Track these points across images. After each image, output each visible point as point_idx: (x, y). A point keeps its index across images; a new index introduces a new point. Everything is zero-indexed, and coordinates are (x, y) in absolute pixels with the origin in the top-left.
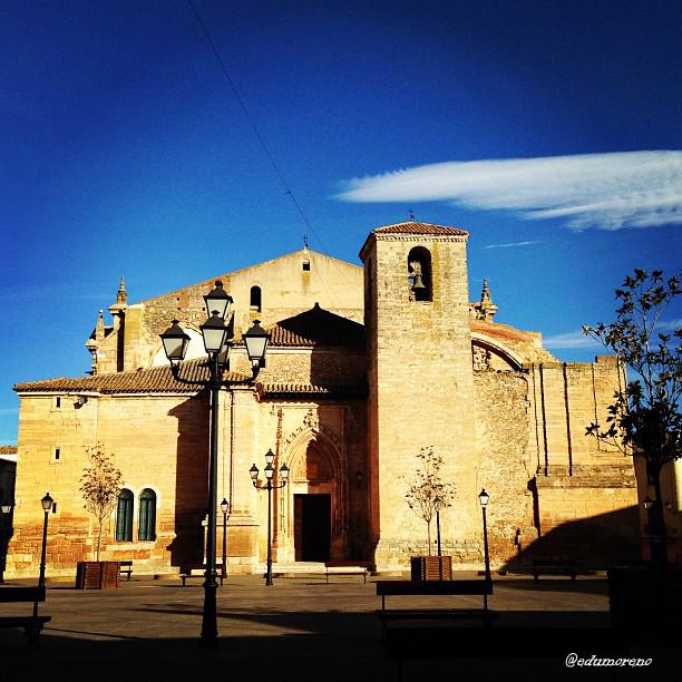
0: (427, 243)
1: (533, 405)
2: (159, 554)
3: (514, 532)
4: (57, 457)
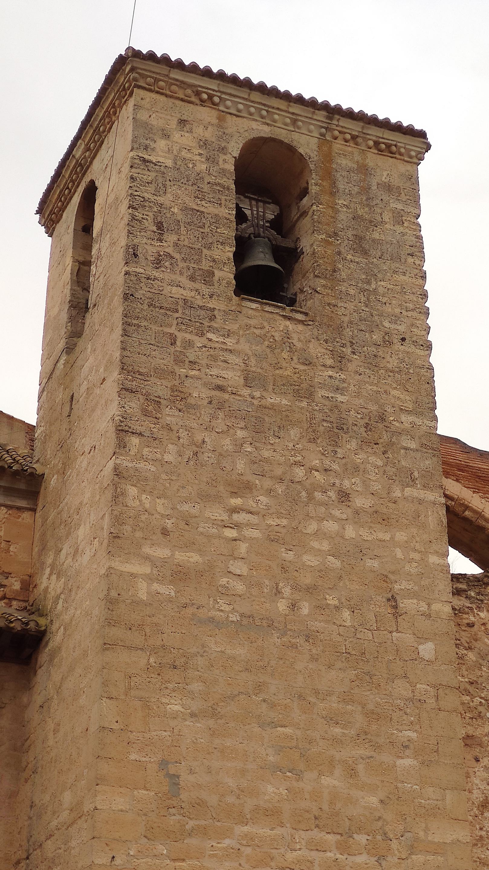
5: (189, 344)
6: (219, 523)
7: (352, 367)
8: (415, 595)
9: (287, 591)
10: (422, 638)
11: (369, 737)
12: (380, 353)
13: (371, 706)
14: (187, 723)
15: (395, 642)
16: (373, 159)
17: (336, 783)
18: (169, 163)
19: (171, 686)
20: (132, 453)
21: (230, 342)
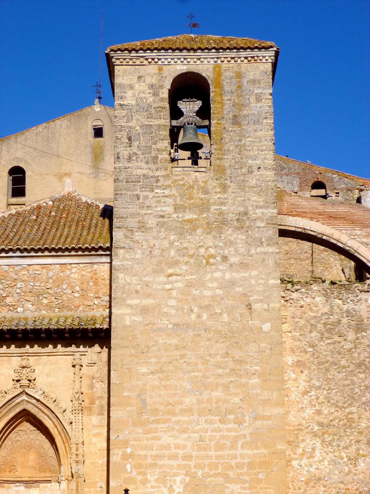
0: (203, 65)
5: (146, 197)
6: (163, 283)
7: (230, 190)
8: (261, 301)
9: (196, 310)
10: (264, 322)
11: (236, 372)
12: (247, 179)
13: (237, 358)
14: (149, 376)
15: (250, 326)
16: (245, 66)
17: (219, 394)
18: (134, 103)
19: (141, 361)
20: (120, 258)
21: (167, 192)
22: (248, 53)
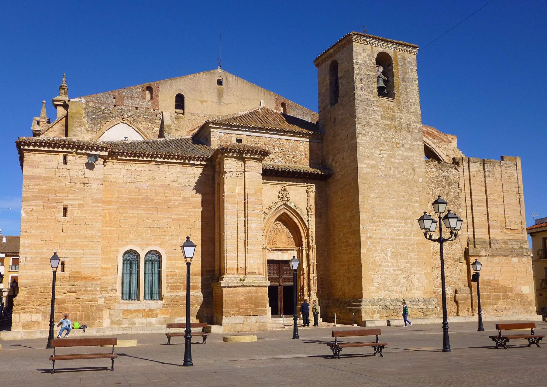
0: (390, 50)
1: (463, 191)
2: (167, 314)
3: (453, 293)
4: (65, 215)
7: (403, 112)
8: (418, 167)
9: (393, 169)
10: (419, 177)
18: (362, 62)
22: (408, 48)
